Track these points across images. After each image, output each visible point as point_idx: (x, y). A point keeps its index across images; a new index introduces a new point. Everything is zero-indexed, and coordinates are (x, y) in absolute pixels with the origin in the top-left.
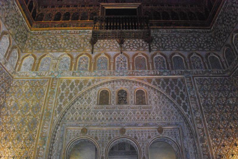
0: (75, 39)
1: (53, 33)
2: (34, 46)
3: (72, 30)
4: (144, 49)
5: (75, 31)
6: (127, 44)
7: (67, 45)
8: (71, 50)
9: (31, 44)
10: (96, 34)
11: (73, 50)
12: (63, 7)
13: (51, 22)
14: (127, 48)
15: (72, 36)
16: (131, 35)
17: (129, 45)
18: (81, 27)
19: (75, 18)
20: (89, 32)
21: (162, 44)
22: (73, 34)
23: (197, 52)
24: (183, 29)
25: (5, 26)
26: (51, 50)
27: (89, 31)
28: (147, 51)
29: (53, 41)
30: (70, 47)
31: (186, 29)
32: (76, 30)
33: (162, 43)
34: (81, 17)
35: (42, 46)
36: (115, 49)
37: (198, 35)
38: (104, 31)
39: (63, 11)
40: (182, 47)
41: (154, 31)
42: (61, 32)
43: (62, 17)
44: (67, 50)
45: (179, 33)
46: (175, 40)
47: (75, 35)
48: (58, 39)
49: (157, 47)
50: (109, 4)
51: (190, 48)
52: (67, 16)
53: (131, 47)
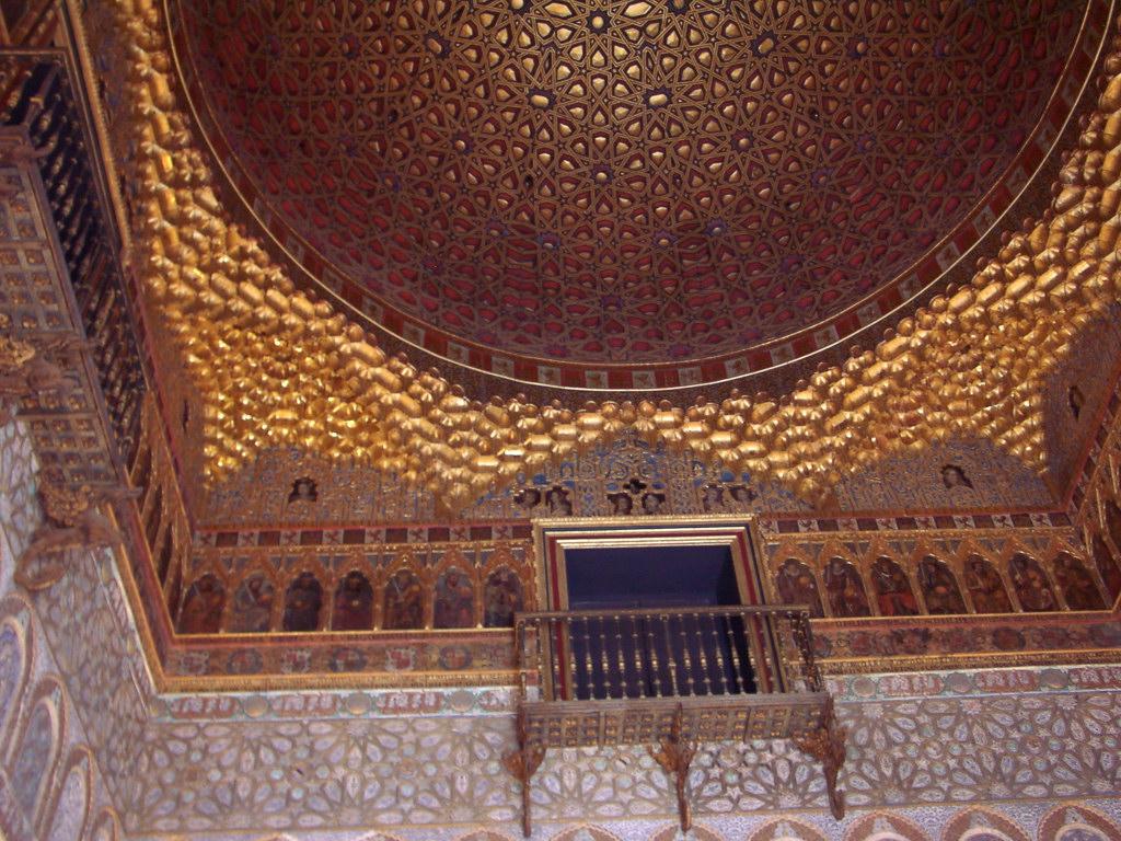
0: (417, 745)
1: (287, 707)
2: (191, 788)
3: (393, 686)
4: (802, 796)
5: (411, 696)
6: (705, 769)
7: (378, 785)
8: (402, 811)
9: (169, 778)
10: (541, 722)
11: (417, 816)
12: (325, 539)
13: (272, 639)
14: (710, 799)
15: (399, 727)
16: (729, 724)
17: (721, 779)
18: (447, 669)
19: (406, 614)
20: (494, 702)
21: (896, 764)
22: (403, 710)
23: (1082, 804)
24: (996, 665)
25: (78, 710)
26: (291, 816)
27: (488, 695)
28: (818, 808)
29: (293, 757)
30: (397, 793)
31: (1011, 665)
32: (414, 685)
33: (893, 758)
34: (438, 605)
35: (233, 787)
36: (647, 804)
37: (1076, 696)
38: (574, 706)
39: (331, 568)
40: (1003, 780)
41: (839, 683)
42: (334, 704)
43: (329, 609)
44: (383, 818)
45: (977, 694)
46: (961, 732)
47: (415, 720)
48: (319, 746)
49: (871, 782)
50: (583, 521)
51: (1043, 784)
52: (356, 604)
53: (730, 791)
